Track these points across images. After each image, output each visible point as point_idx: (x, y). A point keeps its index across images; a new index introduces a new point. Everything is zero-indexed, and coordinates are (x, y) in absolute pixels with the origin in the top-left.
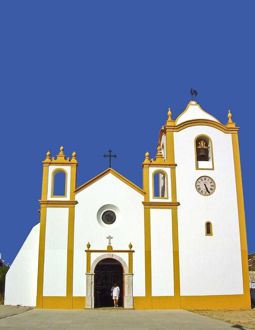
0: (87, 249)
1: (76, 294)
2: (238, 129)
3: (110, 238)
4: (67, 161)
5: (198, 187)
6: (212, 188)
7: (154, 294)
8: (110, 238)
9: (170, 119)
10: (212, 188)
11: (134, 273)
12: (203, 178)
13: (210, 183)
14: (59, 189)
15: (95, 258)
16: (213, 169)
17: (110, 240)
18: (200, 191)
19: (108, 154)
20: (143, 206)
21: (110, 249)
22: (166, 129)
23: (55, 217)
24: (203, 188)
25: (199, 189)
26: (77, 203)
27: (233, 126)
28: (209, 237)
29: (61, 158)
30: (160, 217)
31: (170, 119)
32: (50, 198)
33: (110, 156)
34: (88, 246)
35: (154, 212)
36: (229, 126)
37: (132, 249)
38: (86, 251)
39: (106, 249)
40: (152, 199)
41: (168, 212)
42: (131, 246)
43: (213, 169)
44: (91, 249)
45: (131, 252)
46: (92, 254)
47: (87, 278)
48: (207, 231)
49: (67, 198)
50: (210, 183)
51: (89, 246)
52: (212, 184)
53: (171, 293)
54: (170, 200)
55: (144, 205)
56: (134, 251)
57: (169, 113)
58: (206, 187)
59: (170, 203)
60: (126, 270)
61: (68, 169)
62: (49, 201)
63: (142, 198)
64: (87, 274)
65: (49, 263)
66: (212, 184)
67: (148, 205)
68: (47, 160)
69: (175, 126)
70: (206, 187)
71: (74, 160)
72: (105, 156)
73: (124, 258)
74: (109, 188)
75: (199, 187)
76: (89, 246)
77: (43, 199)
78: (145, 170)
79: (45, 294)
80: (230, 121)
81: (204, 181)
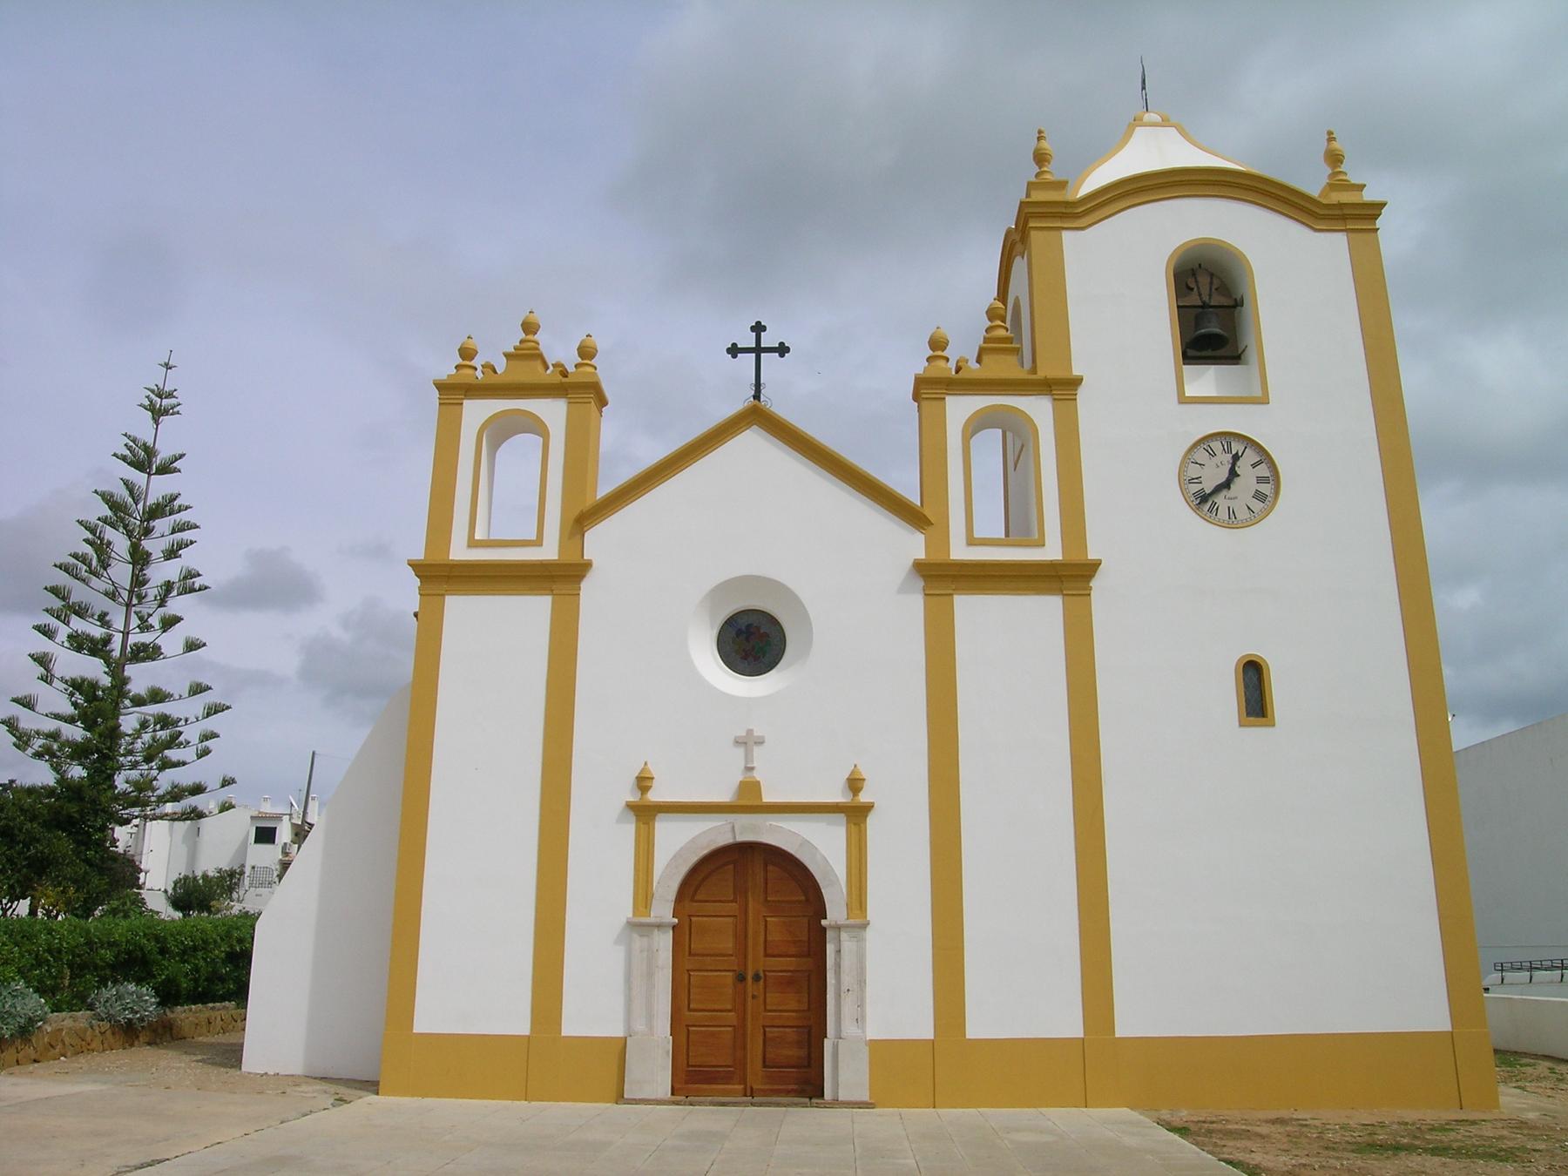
1: (574, 1024)
3: (748, 742)
6: (1266, 489)
7: (977, 1027)
8: (748, 742)
10: (1266, 489)
13: (1254, 466)
16: (1263, 400)
17: (748, 756)
21: (748, 801)
22: (1026, 222)
28: (1257, 734)
30: (1009, 639)
35: (969, 608)
37: (863, 798)
38: (631, 807)
40: (960, 551)
41: (1047, 609)
42: (855, 784)
43: (1263, 400)
44: (654, 796)
45: (856, 814)
48: (1247, 701)
49: (549, 551)
50: (1254, 466)
51: (643, 782)
52: (1263, 470)
53: (1068, 1023)
54: (1052, 551)
56: (866, 809)
59: (1052, 565)
60: (835, 912)
67: (942, 578)
69: (1067, 204)
72: (734, 351)
76: (643, 782)
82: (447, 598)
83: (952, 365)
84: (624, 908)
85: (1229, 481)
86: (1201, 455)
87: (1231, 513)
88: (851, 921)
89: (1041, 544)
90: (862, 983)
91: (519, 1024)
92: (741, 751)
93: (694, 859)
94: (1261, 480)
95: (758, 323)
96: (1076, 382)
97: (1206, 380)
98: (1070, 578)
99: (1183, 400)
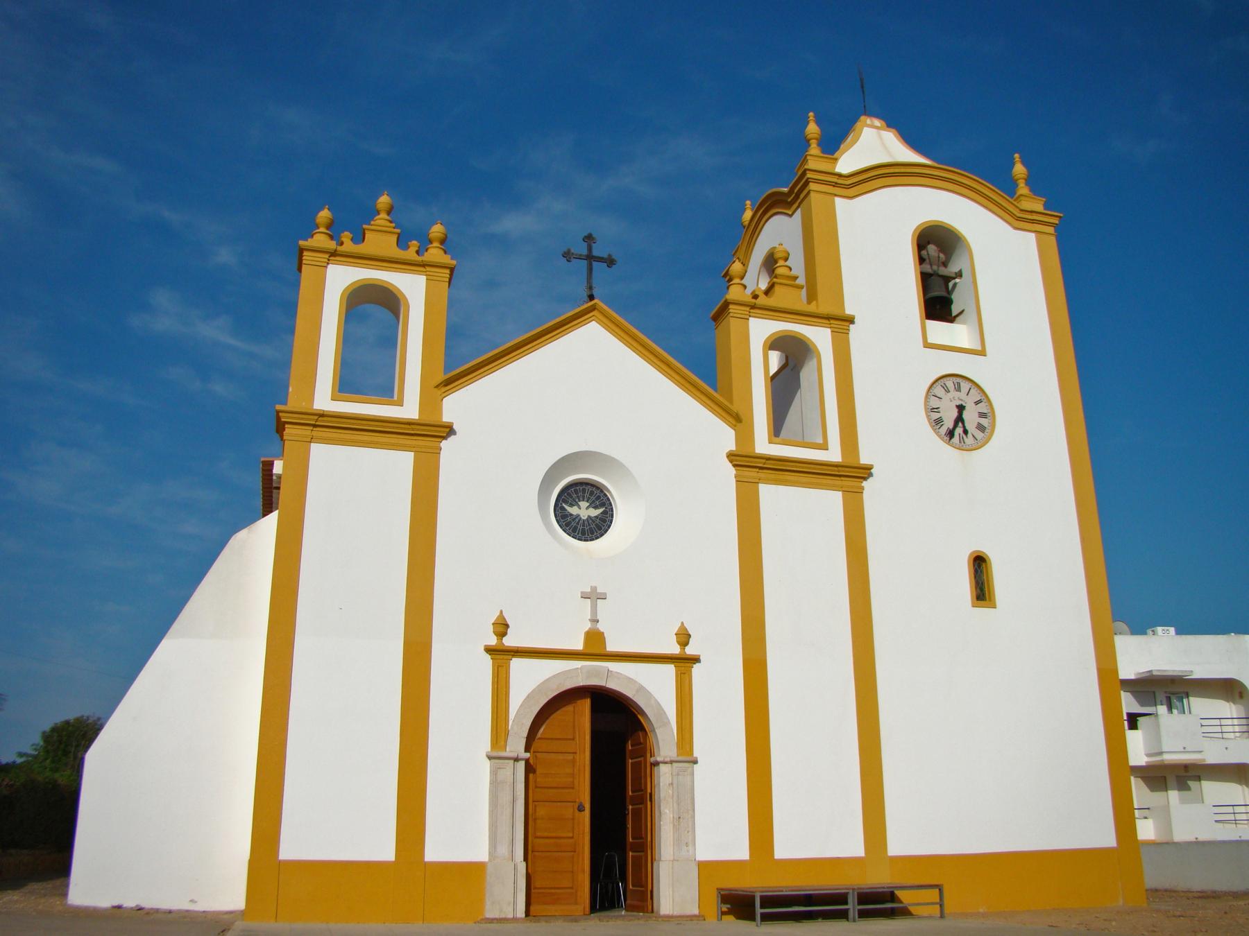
0: (493, 641)
2: (1056, 221)
3: (593, 596)
4: (411, 254)
5: (935, 416)
6: (984, 422)
9: (814, 149)
10: (984, 422)
11: (697, 753)
12: (950, 383)
13: (977, 403)
14: (367, 368)
20: (733, 471)
21: (595, 648)
23: (352, 491)
24: (949, 416)
25: (939, 422)
26: (449, 431)
27: (1039, 207)
29: (380, 240)
30: (801, 521)
31: (814, 149)
32: (324, 399)
33: (590, 258)
34: (501, 629)
36: (1027, 205)
37: (690, 650)
38: (489, 650)
39: (579, 645)
40: (763, 445)
41: (830, 501)
42: (684, 637)
43: (982, 353)
44: (510, 641)
45: (684, 662)
46: (516, 664)
47: (494, 773)
50: (977, 403)
51: (502, 627)
54: (833, 454)
55: (735, 466)
57: (812, 129)
58: (961, 418)
61: (412, 287)
62: (322, 415)
63: (727, 438)
64: (495, 754)
65: (291, 702)
66: (982, 408)
68: (320, 240)
70: (961, 418)
71: (435, 253)
73: (653, 688)
74: (587, 384)
76: (502, 627)
77: (294, 403)
78: (733, 323)
79: (288, 851)
80: (1023, 189)
81: (953, 393)
82: (312, 445)
83: (749, 291)
84: (486, 745)
86: (938, 390)
88: (680, 758)
89: (824, 446)
91: (385, 851)
94: (982, 415)
96: (851, 320)
97: (939, 330)
98: (849, 475)
99: (927, 345)
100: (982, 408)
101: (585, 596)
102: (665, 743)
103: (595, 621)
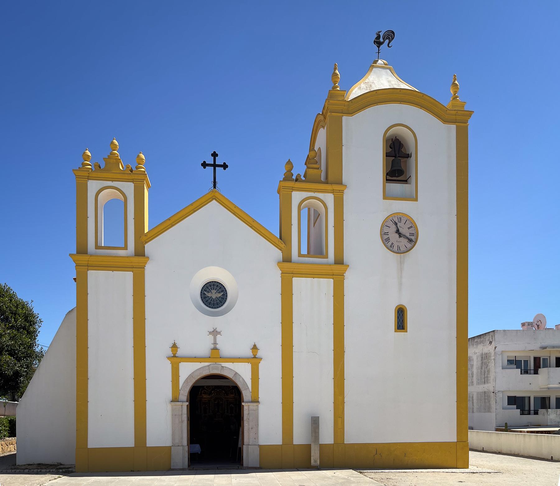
8: (215, 333)
13: (409, 228)
15: (189, 372)
17: (215, 339)
18: (390, 244)
19: (210, 161)
25: (388, 240)
28: (401, 334)
33: (215, 166)
50: (409, 228)
72: (204, 165)
73: (241, 372)
75: (387, 236)
85: (400, 236)
87: (399, 247)
90: (257, 425)
92: (211, 337)
93: (194, 381)
95: (215, 152)
100: (412, 231)
101: (210, 333)
102: (246, 395)
103: (215, 343)
